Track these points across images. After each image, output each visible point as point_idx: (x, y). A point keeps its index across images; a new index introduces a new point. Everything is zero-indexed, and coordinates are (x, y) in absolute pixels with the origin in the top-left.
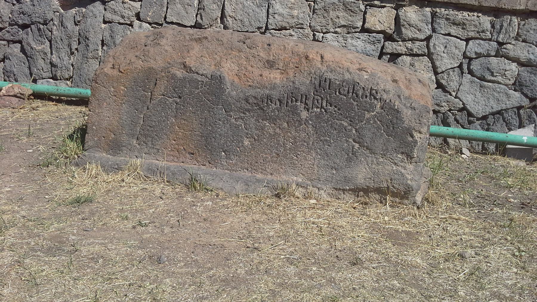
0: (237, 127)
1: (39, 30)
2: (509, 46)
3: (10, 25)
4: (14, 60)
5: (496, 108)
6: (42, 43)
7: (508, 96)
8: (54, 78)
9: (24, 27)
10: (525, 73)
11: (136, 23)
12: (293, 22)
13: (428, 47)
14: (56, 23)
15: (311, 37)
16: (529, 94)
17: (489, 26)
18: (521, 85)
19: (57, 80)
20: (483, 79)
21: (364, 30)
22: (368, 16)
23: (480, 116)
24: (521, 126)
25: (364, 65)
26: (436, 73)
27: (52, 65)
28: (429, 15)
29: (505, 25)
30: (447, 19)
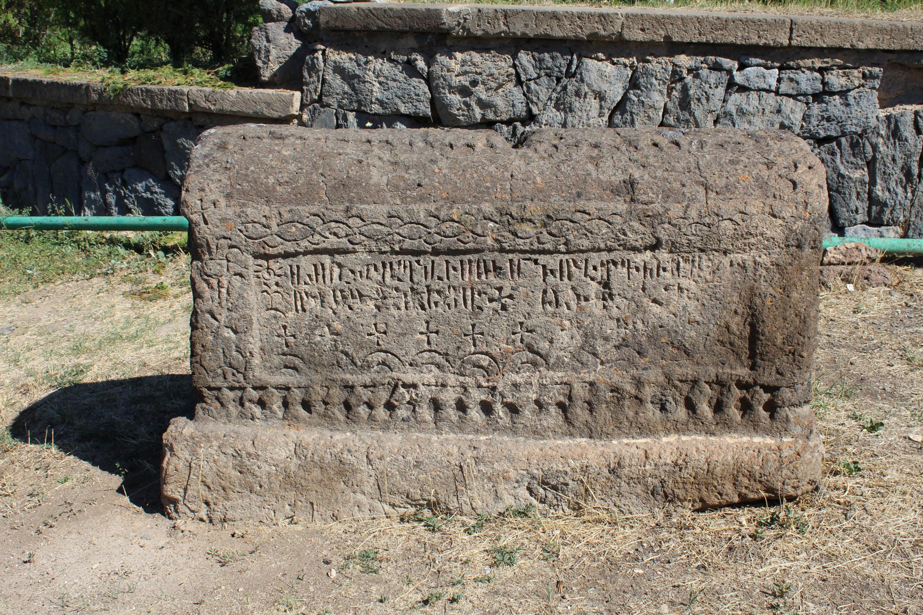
1: (854, 145)
14: (883, 132)
19: (880, 225)
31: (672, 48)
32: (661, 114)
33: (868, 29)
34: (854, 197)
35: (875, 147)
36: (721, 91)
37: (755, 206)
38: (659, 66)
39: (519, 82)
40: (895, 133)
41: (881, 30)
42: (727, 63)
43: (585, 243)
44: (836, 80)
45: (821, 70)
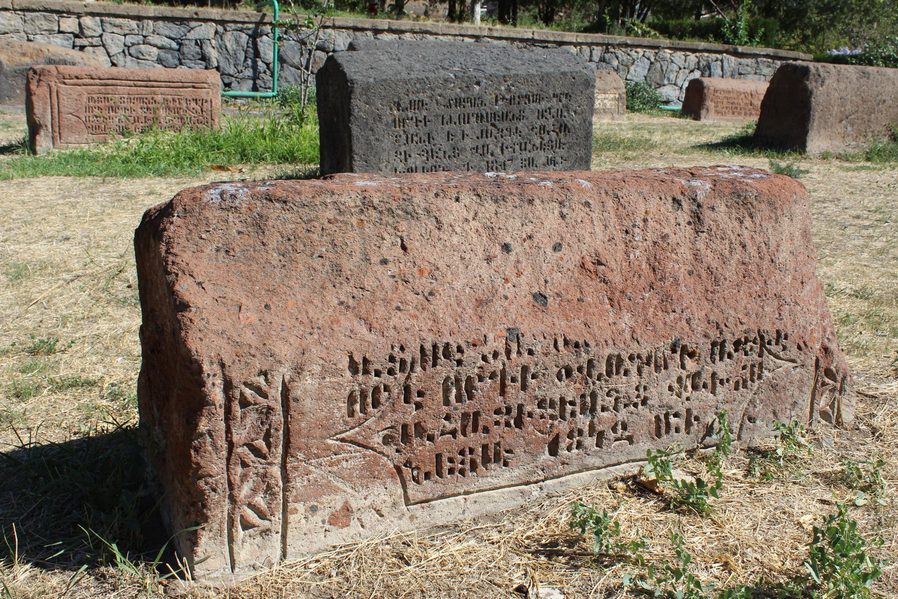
0: (13, 85)
2: (150, 38)
10: (162, 54)
12: (12, 28)
13: (102, 41)
15: (26, 38)
17: (136, 27)
18: (161, 60)
20: (138, 58)
21: (60, 32)
22: (61, 23)
25: (68, 52)
26: (110, 56)
28: (99, 21)
29: (145, 25)
30: (110, 24)
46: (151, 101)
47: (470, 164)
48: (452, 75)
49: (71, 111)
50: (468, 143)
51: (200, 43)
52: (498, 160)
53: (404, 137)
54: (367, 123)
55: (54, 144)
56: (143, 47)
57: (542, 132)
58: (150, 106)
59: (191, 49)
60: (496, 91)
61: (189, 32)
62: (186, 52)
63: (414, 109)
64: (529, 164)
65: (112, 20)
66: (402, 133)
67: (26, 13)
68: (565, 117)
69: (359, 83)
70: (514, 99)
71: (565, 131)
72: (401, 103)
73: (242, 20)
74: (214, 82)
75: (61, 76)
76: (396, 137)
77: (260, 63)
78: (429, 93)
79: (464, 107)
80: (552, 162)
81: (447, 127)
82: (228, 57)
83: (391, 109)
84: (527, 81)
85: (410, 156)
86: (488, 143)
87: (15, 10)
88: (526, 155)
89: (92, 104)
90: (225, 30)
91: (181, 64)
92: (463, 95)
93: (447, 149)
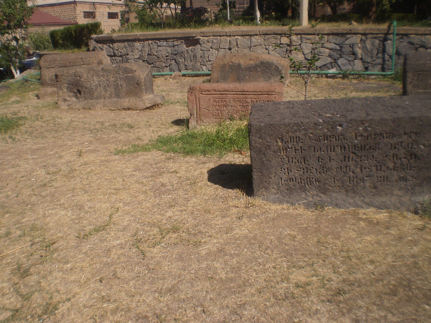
0: (245, 74)
1: (181, 55)
2: (325, 44)
3: (171, 54)
4: (173, 66)
5: (324, 64)
6: (182, 59)
7: (327, 60)
8: (186, 69)
9: (176, 55)
10: (332, 53)
11: (211, 49)
12: (258, 44)
16: (334, 58)
23: (319, 66)
24: (332, 68)
26: (304, 55)
27: (185, 65)
31: (148, 40)
32: (147, 52)
33: (178, 34)
34: (182, 65)
35: (184, 55)
36: (157, 47)
37: (93, 59)
38: (146, 43)
39: (126, 48)
40: (188, 52)
41: (181, 34)
42: (157, 41)
43: (77, 65)
44: (176, 43)
45: (173, 42)
46: (245, 102)
47: (336, 178)
48: (321, 121)
49: (205, 107)
50: (334, 164)
51: (352, 46)
52: (358, 176)
53: (286, 159)
54: (261, 151)
55: (197, 123)
56: (321, 49)
57: (395, 158)
58: (244, 104)
59: (347, 49)
60: (356, 131)
61: (346, 40)
62: (344, 51)
63: (293, 142)
64: (384, 181)
65: (306, 36)
66: (285, 157)
67: (265, 36)
68: (415, 148)
69: (255, 126)
70: (371, 136)
71: (415, 158)
72: (284, 138)
73: (376, 32)
74: (279, 91)
75: (201, 90)
76: (281, 159)
77: (386, 56)
78: (303, 132)
79: (330, 141)
80: (404, 179)
81: (317, 154)
82: (368, 53)
83: (277, 142)
84: (382, 124)
85: (291, 171)
86: (349, 165)
87: (260, 35)
88: (380, 174)
89: (215, 104)
90: (367, 38)
91: (341, 57)
92: (329, 134)
93: (318, 168)
